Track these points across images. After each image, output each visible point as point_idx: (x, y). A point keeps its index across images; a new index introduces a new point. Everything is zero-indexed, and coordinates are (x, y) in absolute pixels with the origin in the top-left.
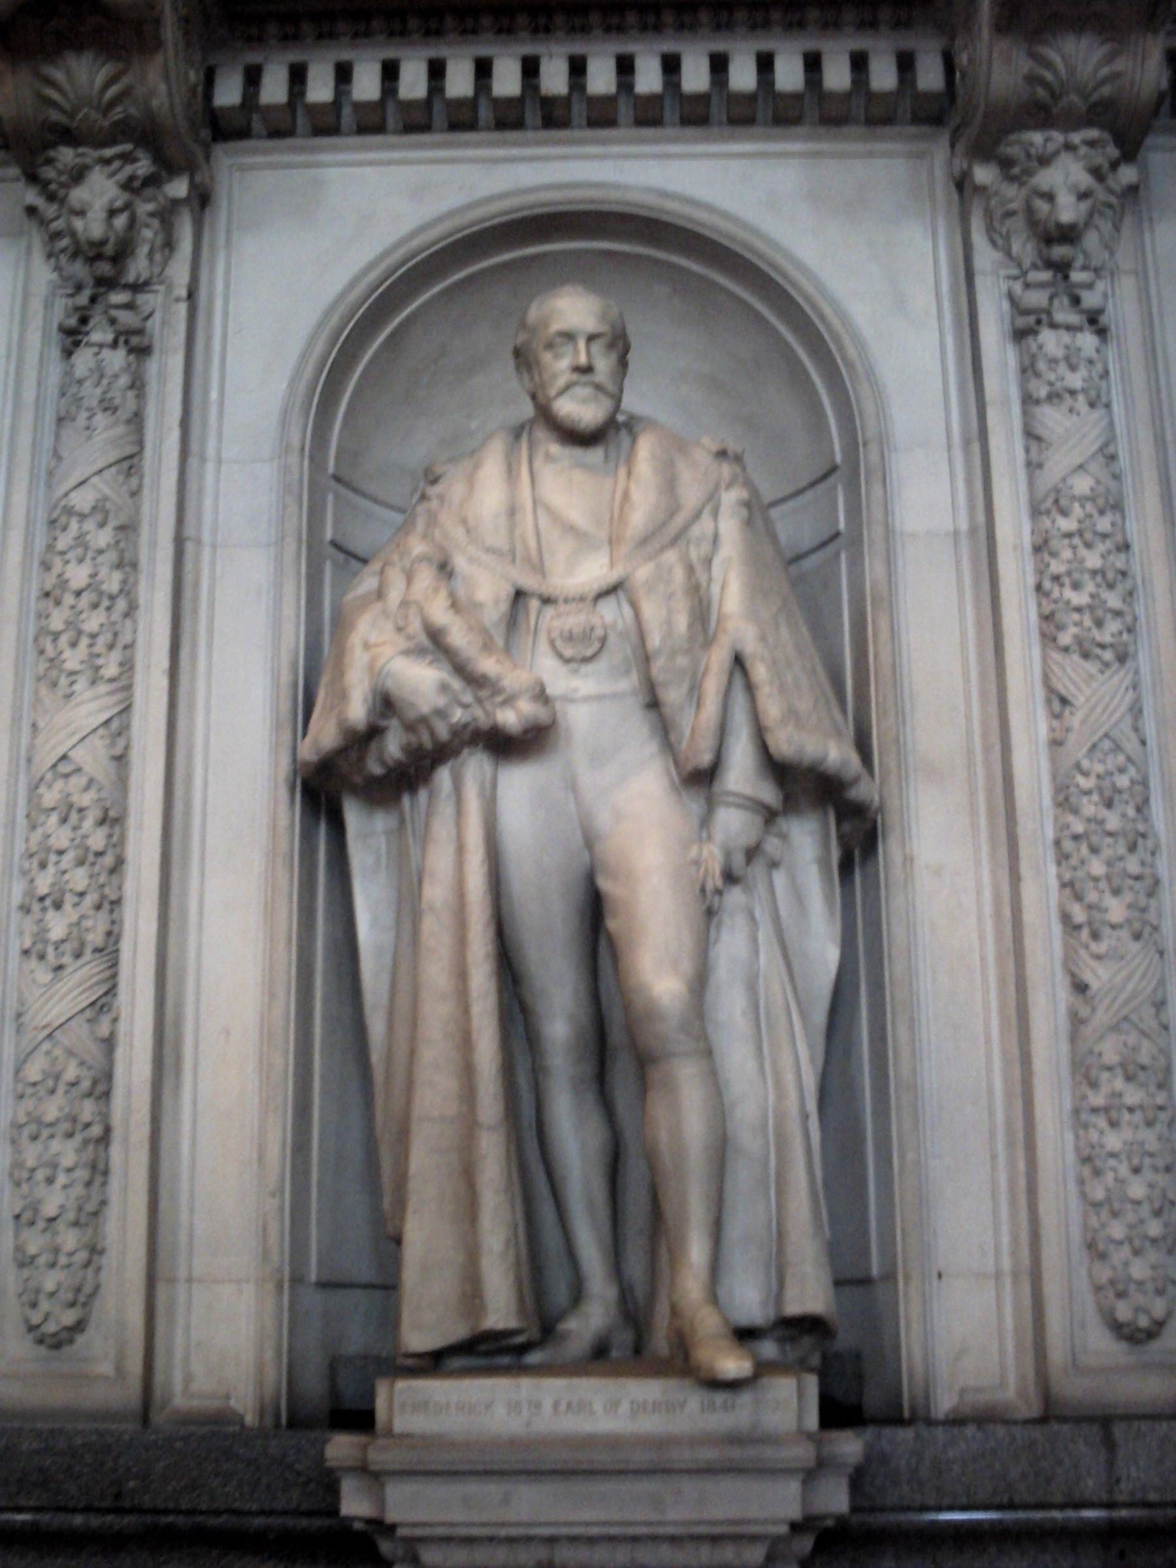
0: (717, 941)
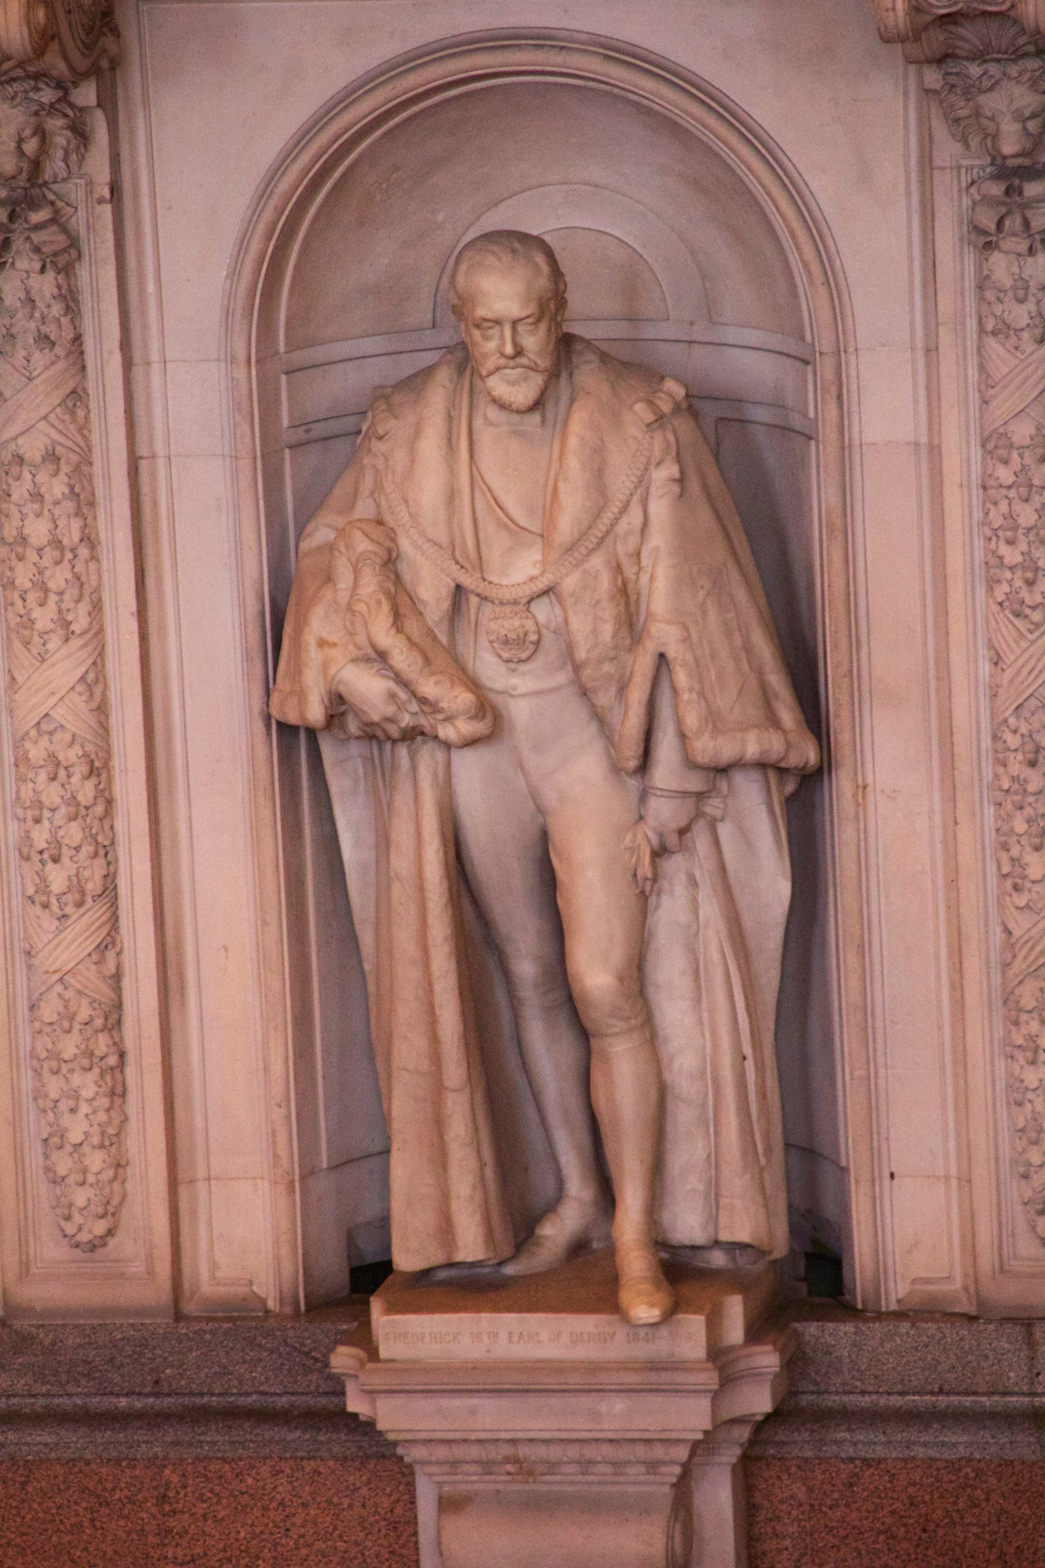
0: (657, 907)
